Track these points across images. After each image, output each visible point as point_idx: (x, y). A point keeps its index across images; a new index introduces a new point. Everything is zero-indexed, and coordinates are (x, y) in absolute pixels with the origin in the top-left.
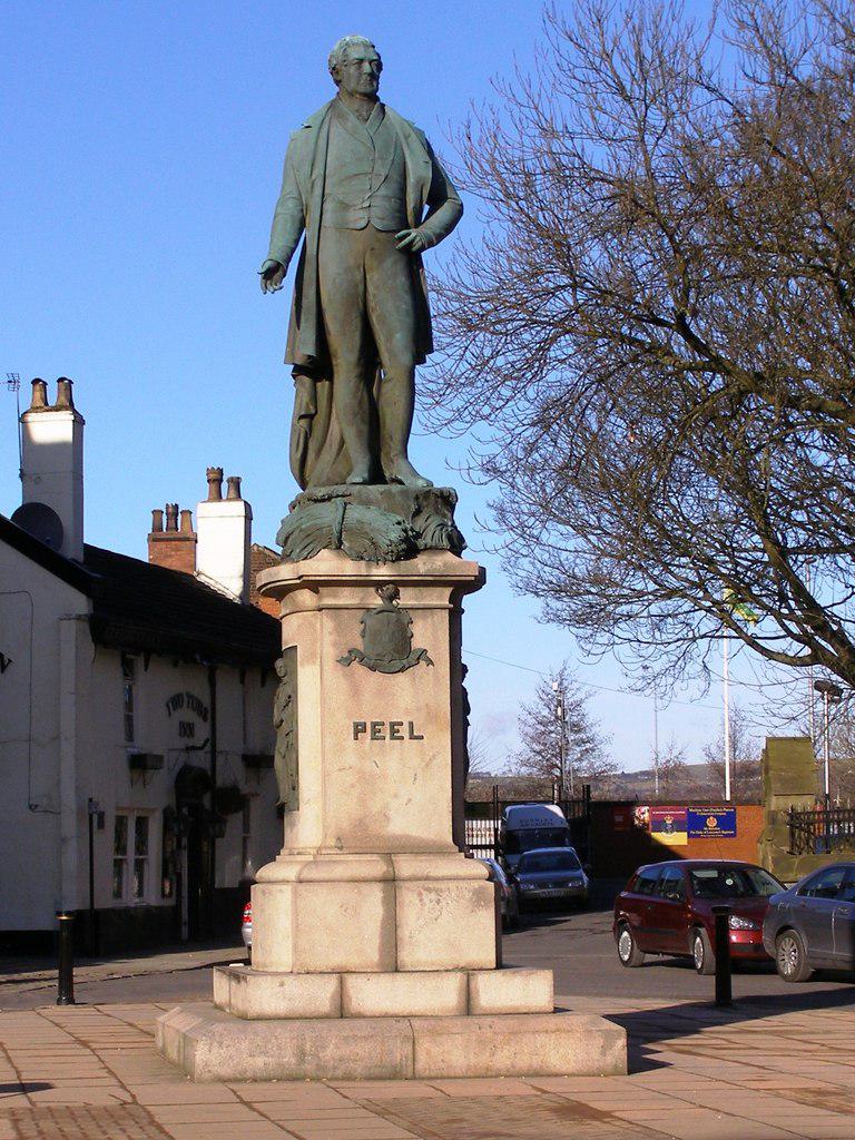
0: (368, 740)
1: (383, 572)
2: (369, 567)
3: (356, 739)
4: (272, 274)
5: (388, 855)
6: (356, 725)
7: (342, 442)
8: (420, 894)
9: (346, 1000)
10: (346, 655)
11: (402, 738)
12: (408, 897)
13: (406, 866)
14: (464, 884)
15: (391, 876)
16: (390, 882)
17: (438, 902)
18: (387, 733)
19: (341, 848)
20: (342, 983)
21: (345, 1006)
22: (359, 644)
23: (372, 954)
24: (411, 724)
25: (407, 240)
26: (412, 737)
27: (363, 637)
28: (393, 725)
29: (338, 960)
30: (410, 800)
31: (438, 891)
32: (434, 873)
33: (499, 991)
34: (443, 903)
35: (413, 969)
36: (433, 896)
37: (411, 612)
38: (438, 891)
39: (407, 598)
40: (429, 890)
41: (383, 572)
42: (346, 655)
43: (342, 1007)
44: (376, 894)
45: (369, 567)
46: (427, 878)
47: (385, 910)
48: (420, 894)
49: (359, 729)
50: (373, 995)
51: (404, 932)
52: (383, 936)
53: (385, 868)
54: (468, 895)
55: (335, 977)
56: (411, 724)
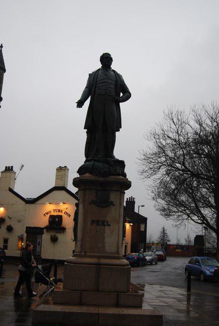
1: (102, 179)
4: (80, 104)
6: (92, 221)
18: (100, 223)
41: (102, 179)
49: (93, 222)
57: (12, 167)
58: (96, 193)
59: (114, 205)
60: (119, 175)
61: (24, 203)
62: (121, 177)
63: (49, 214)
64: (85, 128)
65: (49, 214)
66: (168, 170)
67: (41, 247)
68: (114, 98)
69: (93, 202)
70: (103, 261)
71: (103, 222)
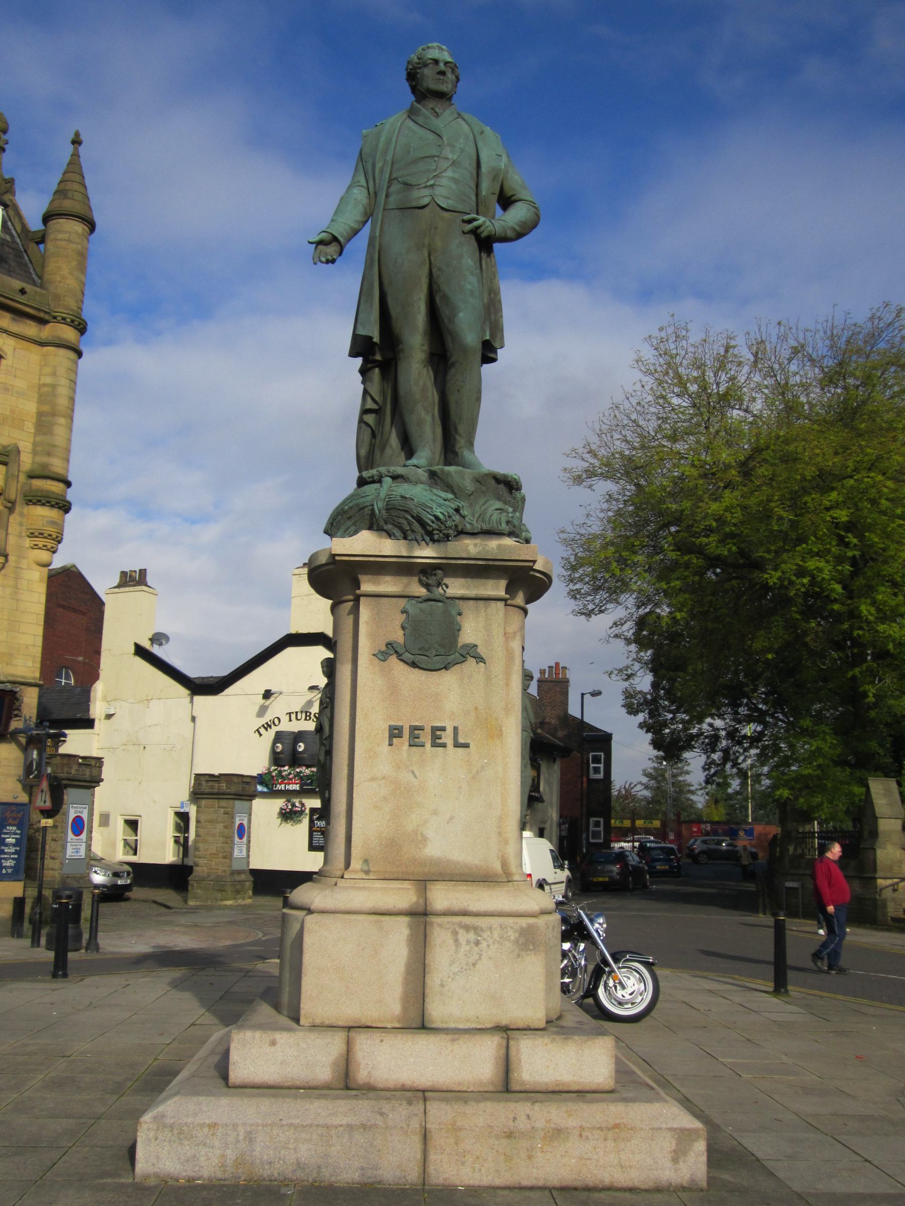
0: (406, 747)
1: (426, 553)
2: (410, 548)
5: (423, 883)
8: (455, 933)
10: (384, 648)
11: (444, 746)
12: (440, 935)
13: (442, 897)
14: (510, 921)
15: (421, 909)
16: (420, 916)
17: (477, 943)
19: (367, 872)
20: (349, 1043)
21: (351, 1074)
22: (398, 636)
23: (390, 1003)
25: (475, 224)
26: (457, 745)
28: (435, 729)
29: (349, 1010)
30: (452, 818)
32: (474, 907)
33: (546, 1061)
36: (472, 936)
37: (461, 602)
38: (476, 929)
39: (456, 587)
40: (467, 928)
41: (426, 553)
42: (384, 648)
44: (401, 929)
45: (410, 548)
46: (465, 913)
47: (410, 951)
48: (455, 933)
49: (395, 733)
50: (390, 1060)
51: (433, 981)
52: (407, 982)
53: (414, 899)
54: (513, 935)
56: (456, 729)
57: (143, 572)
58: (404, 611)
59: (480, 659)
60: (499, 534)
61: (184, 692)
62: (508, 541)
63: (274, 729)
64: (353, 354)
65: (274, 729)
66: (741, 434)
67: (249, 842)
68: (470, 221)
71: (436, 732)
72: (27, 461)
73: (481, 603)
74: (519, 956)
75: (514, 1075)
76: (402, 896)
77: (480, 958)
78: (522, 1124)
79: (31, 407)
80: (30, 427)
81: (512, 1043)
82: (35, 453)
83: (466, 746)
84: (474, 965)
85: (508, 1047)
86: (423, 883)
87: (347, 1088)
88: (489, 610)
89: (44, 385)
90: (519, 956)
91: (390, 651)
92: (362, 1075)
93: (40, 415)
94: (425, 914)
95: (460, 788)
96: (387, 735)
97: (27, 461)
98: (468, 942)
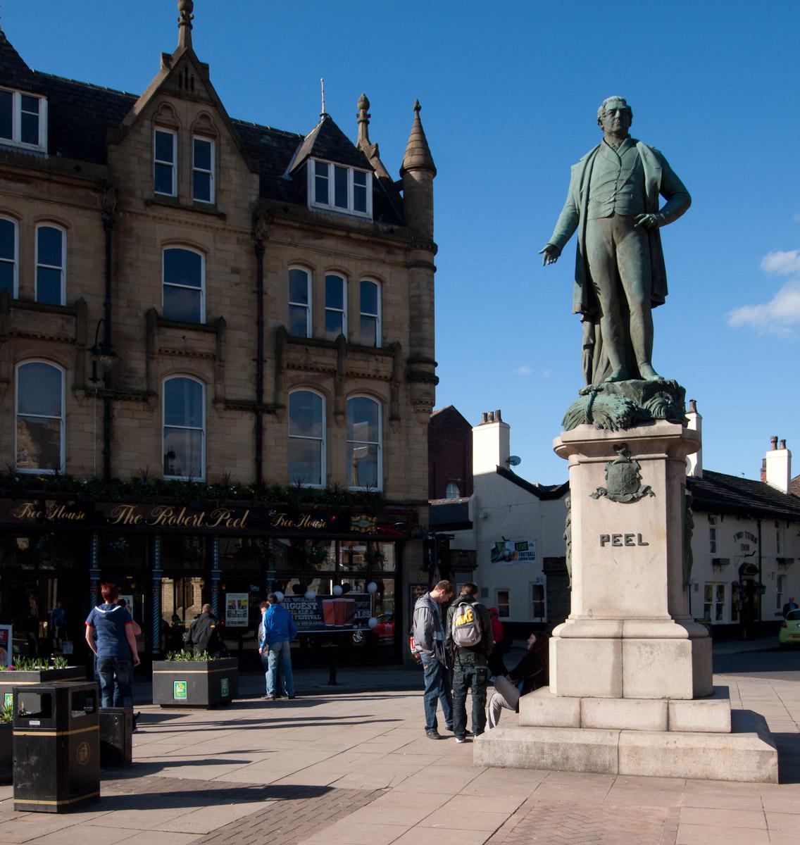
1: (617, 435)
2: (606, 433)
3: (603, 545)
6: (603, 537)
7: (609, 363)
8: (639, 648)
9: (583, 716)
11: (634, 545)
12: (631, 648)
15: (620, 636)
17: (652, 653)
18: (623, 541)
19: (591, 616)
21: (583, 720)
22: (603, 484)
24: (640, 536)
27: (607, 479)
28: (627, 536)
29: (582, 690)
30: (638, 585)
31: (651, 645)
32: (650, 633)
34: (655, 654)
35: (635, 697)
36: (648, 649)
38: (651, 645)
40: (645, 645)
43: (580, 721)
44: (609, 646)
45: (606, 433)
49: (604, 540)
53: (617, 629)
54: (673, 649)
55: (578, 700)
56: (640, 536)
69: (600, 493)
70: (631, 629)
71: (628, 538)
72: (406, 351)
73: (651, 461)
74: (676, 659)
75: (671, 723)
76: (612, 629)
77: (654, 661)
78: (672, 746)
79: (404, 314)
80: (406, 327)
81: (670, 706)
82: (411, 345)
83: (647, 544)
84: (650, 665)
85: (668, 708)
86: (622, 621)
87: (580, 727)
88: (656, 465)
89: (414, 296)
90: (676, 659)
91: (600, 493)
92: (588, 720)
93: (412, 318)
94: (622, 638)
95: (642, 568)
96: (599, 540)
97: (406, 351)
98: (647, 652)
